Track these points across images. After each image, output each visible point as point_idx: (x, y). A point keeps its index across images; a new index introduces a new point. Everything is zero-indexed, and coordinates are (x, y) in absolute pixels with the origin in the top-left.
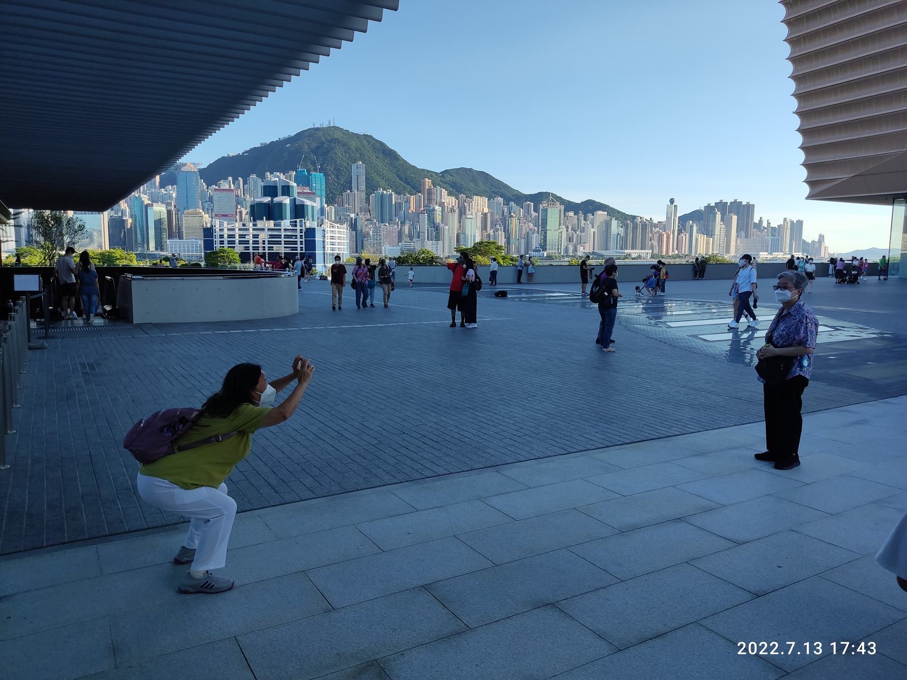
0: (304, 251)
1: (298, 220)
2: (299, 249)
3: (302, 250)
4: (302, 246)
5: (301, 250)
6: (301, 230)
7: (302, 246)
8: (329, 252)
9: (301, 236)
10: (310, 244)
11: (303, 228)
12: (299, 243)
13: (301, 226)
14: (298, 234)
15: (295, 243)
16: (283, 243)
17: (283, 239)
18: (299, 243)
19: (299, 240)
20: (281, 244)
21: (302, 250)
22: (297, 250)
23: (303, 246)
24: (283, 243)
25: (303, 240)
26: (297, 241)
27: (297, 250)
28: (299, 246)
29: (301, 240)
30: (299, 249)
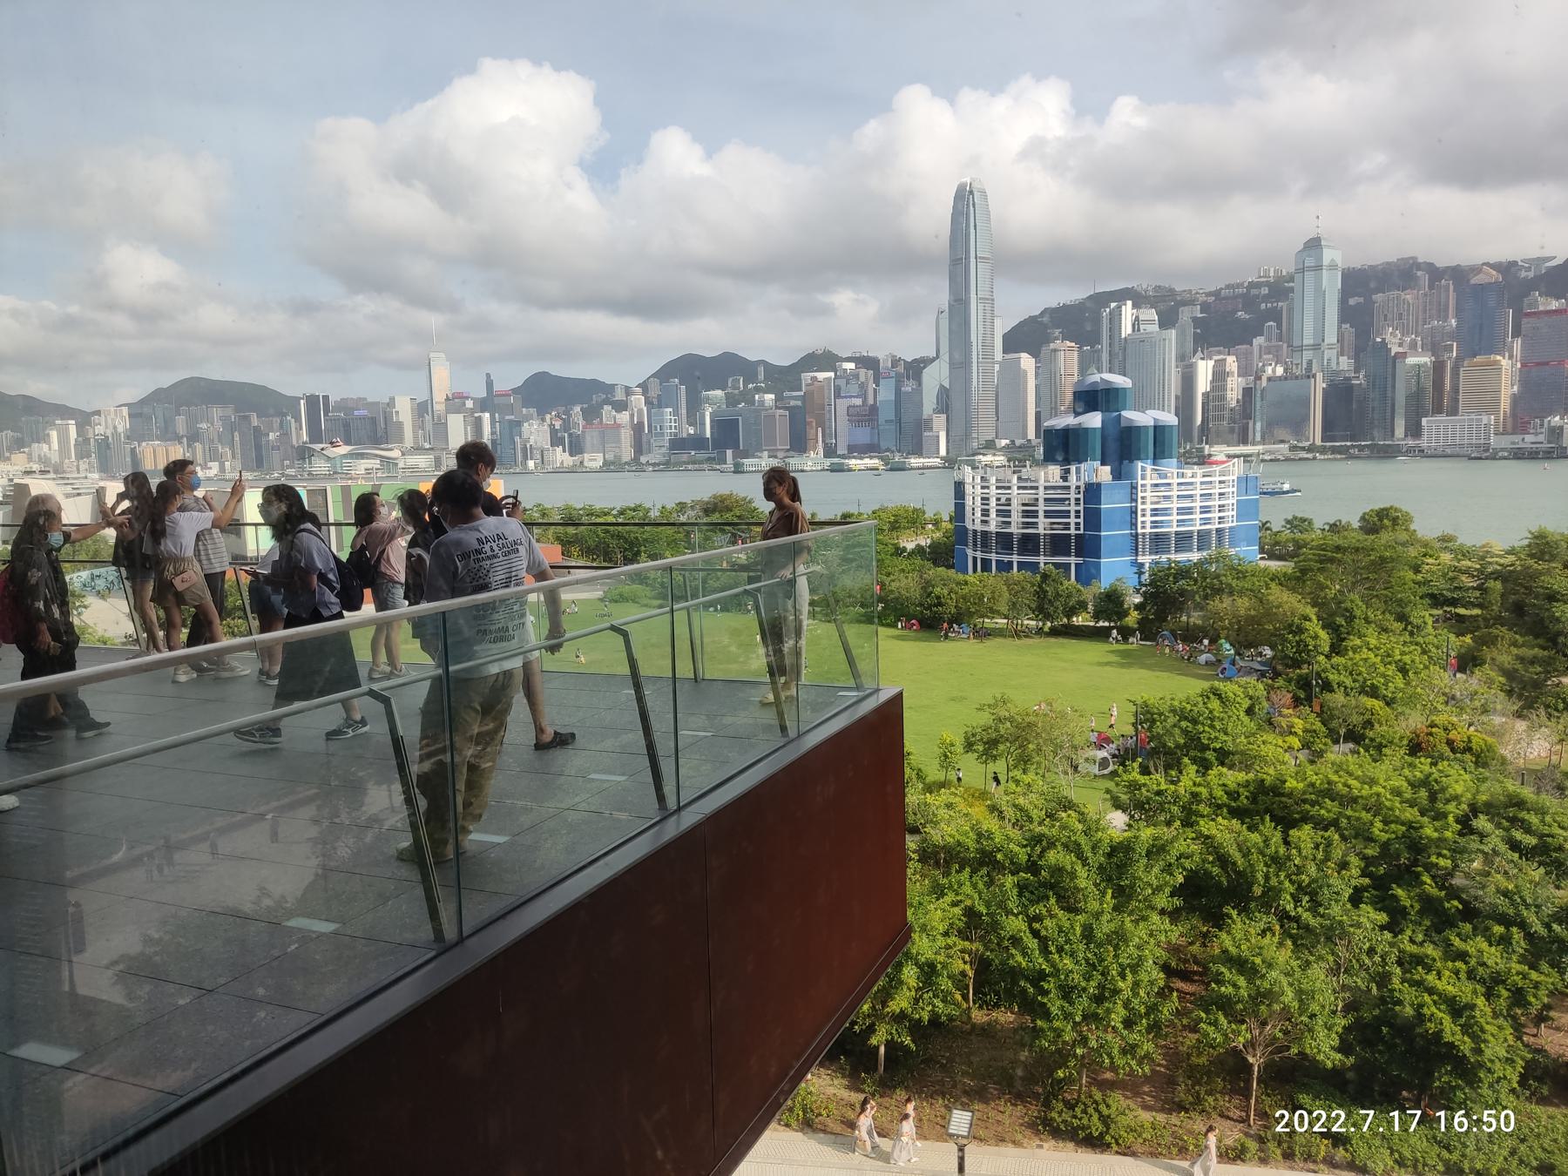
0: (1082, 532)
1: (1073, 468)
2: (1073, 526)
3: (1079, 529)
4: (1078, 520)
5: (1077, 529)
6: (1078, 487)
7: (1078, 520)
8: (1148, 530)
9: (1077, 500)
10: (1093, 518)
11: (1081, 484)
12: (1073, 514)
13: (1078, 479)
14: (1073, 496)
15: (1066, 514)
16: (1041, 514)
17: (1041, 508)
18: (1073, 514)
19: (1073, 508)
20: (1037, 517)
21: (1079, 529)
22: (1069, 529)
23: (1081, 520)
24: (1041, 514)
25: (1081, 508)
26: (1069, 512)
27: (1069, 529)
28: (1072, 520)
29: (1078, 508)
30: (1073, 526)
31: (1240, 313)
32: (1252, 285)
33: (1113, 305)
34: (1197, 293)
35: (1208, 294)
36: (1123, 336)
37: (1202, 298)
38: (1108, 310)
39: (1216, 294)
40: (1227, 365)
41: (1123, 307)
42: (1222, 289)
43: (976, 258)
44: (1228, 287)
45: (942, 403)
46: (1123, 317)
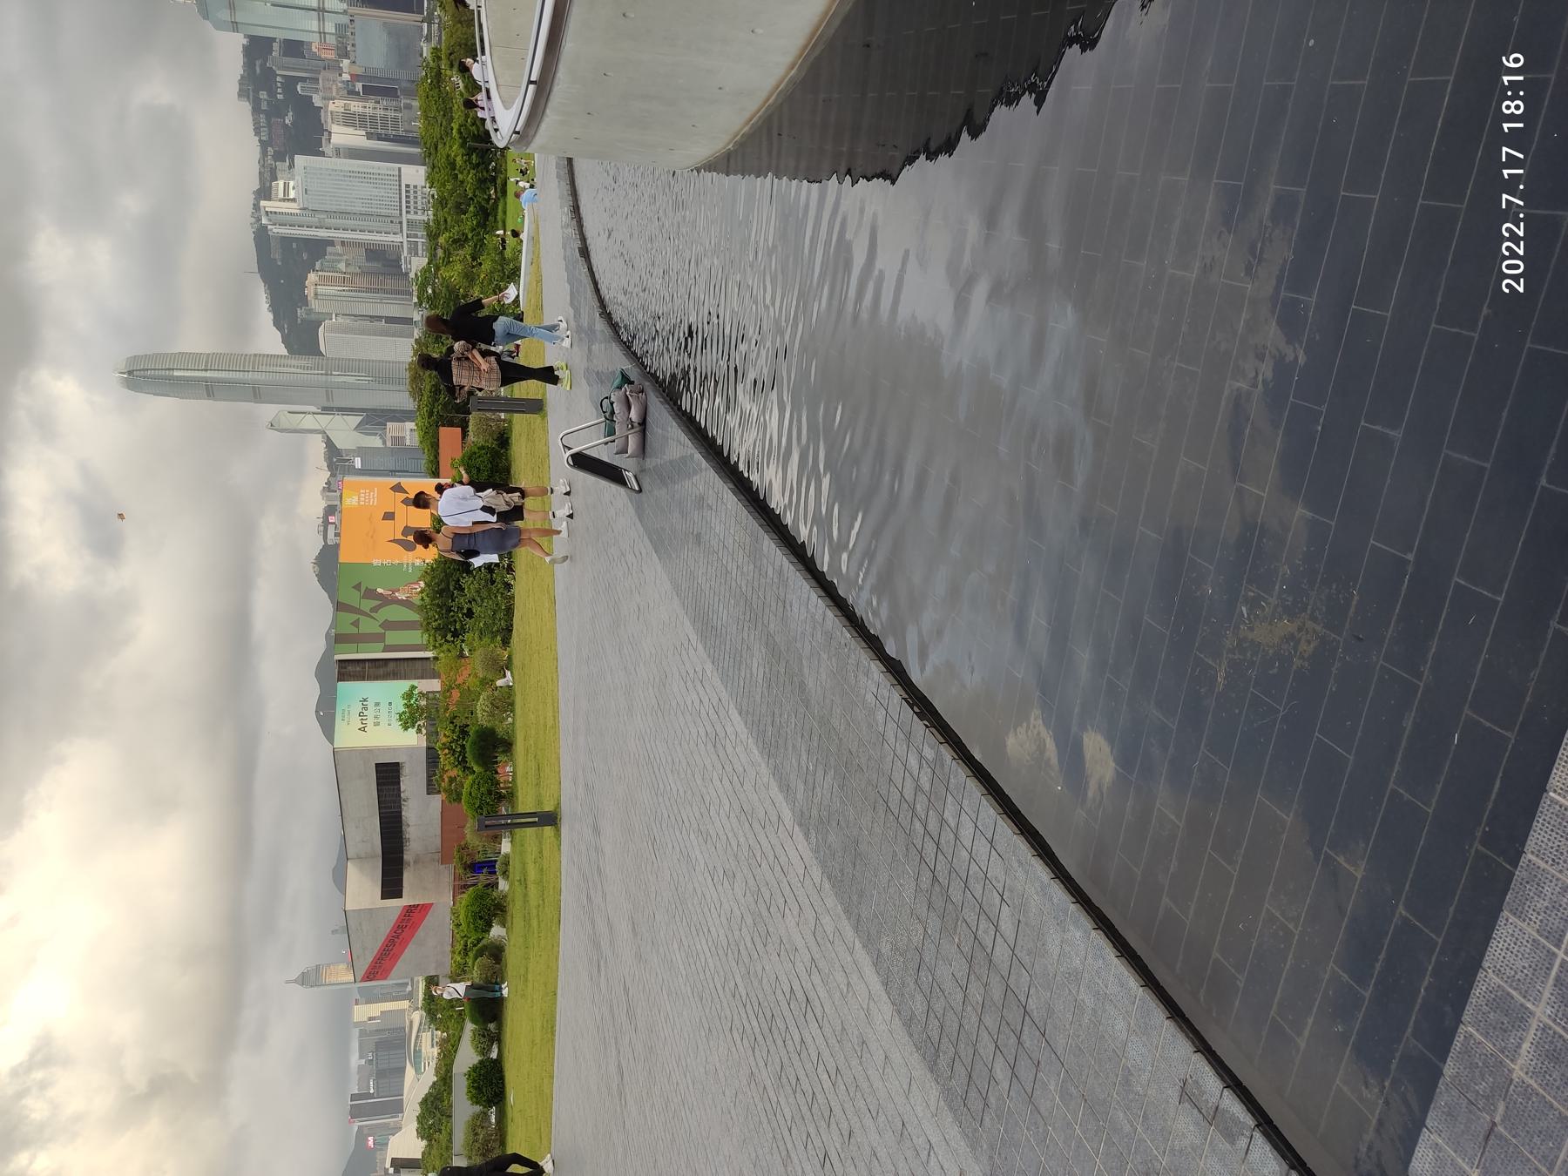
31: (287, 121)
32: (256, 110)
33: (264, 221)
34: (263, 166)
35: (264, 153)
36: (298, 211)
37: (270, 161)
38: (269, 227)
39: (264, 145)
40: (337, 110)
41: (267, 209)
42: (260, 141)
43: (206, 370)
44: (257, 131)
45: (375, 429)
46: (277, 210)
